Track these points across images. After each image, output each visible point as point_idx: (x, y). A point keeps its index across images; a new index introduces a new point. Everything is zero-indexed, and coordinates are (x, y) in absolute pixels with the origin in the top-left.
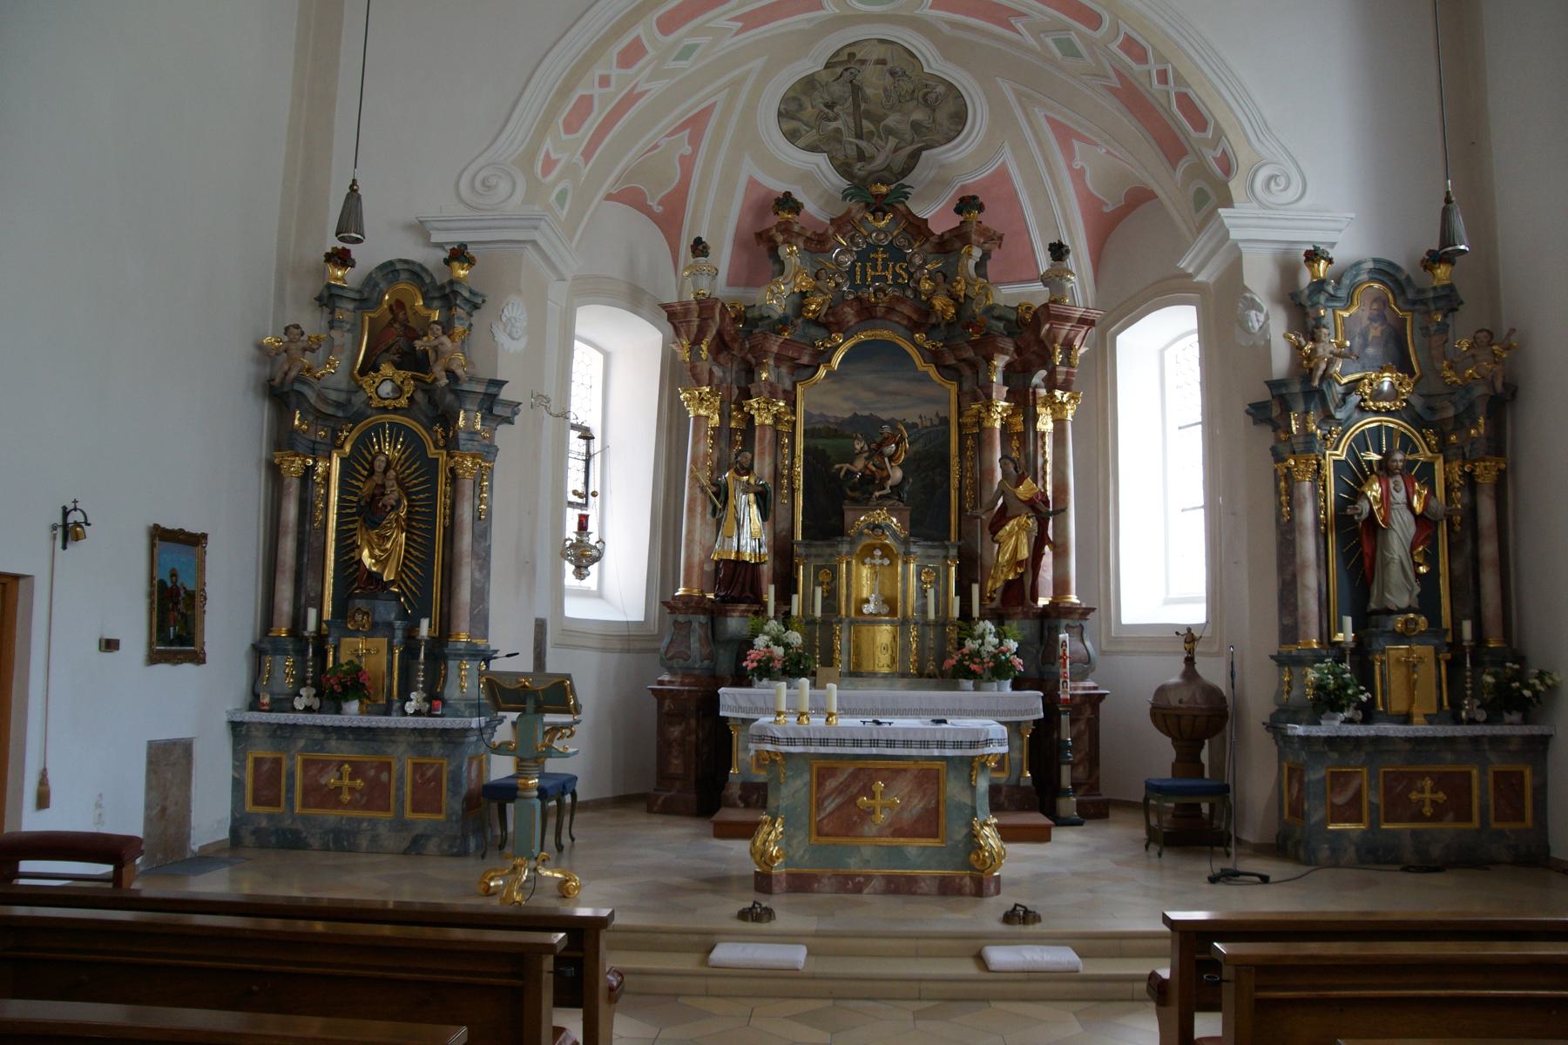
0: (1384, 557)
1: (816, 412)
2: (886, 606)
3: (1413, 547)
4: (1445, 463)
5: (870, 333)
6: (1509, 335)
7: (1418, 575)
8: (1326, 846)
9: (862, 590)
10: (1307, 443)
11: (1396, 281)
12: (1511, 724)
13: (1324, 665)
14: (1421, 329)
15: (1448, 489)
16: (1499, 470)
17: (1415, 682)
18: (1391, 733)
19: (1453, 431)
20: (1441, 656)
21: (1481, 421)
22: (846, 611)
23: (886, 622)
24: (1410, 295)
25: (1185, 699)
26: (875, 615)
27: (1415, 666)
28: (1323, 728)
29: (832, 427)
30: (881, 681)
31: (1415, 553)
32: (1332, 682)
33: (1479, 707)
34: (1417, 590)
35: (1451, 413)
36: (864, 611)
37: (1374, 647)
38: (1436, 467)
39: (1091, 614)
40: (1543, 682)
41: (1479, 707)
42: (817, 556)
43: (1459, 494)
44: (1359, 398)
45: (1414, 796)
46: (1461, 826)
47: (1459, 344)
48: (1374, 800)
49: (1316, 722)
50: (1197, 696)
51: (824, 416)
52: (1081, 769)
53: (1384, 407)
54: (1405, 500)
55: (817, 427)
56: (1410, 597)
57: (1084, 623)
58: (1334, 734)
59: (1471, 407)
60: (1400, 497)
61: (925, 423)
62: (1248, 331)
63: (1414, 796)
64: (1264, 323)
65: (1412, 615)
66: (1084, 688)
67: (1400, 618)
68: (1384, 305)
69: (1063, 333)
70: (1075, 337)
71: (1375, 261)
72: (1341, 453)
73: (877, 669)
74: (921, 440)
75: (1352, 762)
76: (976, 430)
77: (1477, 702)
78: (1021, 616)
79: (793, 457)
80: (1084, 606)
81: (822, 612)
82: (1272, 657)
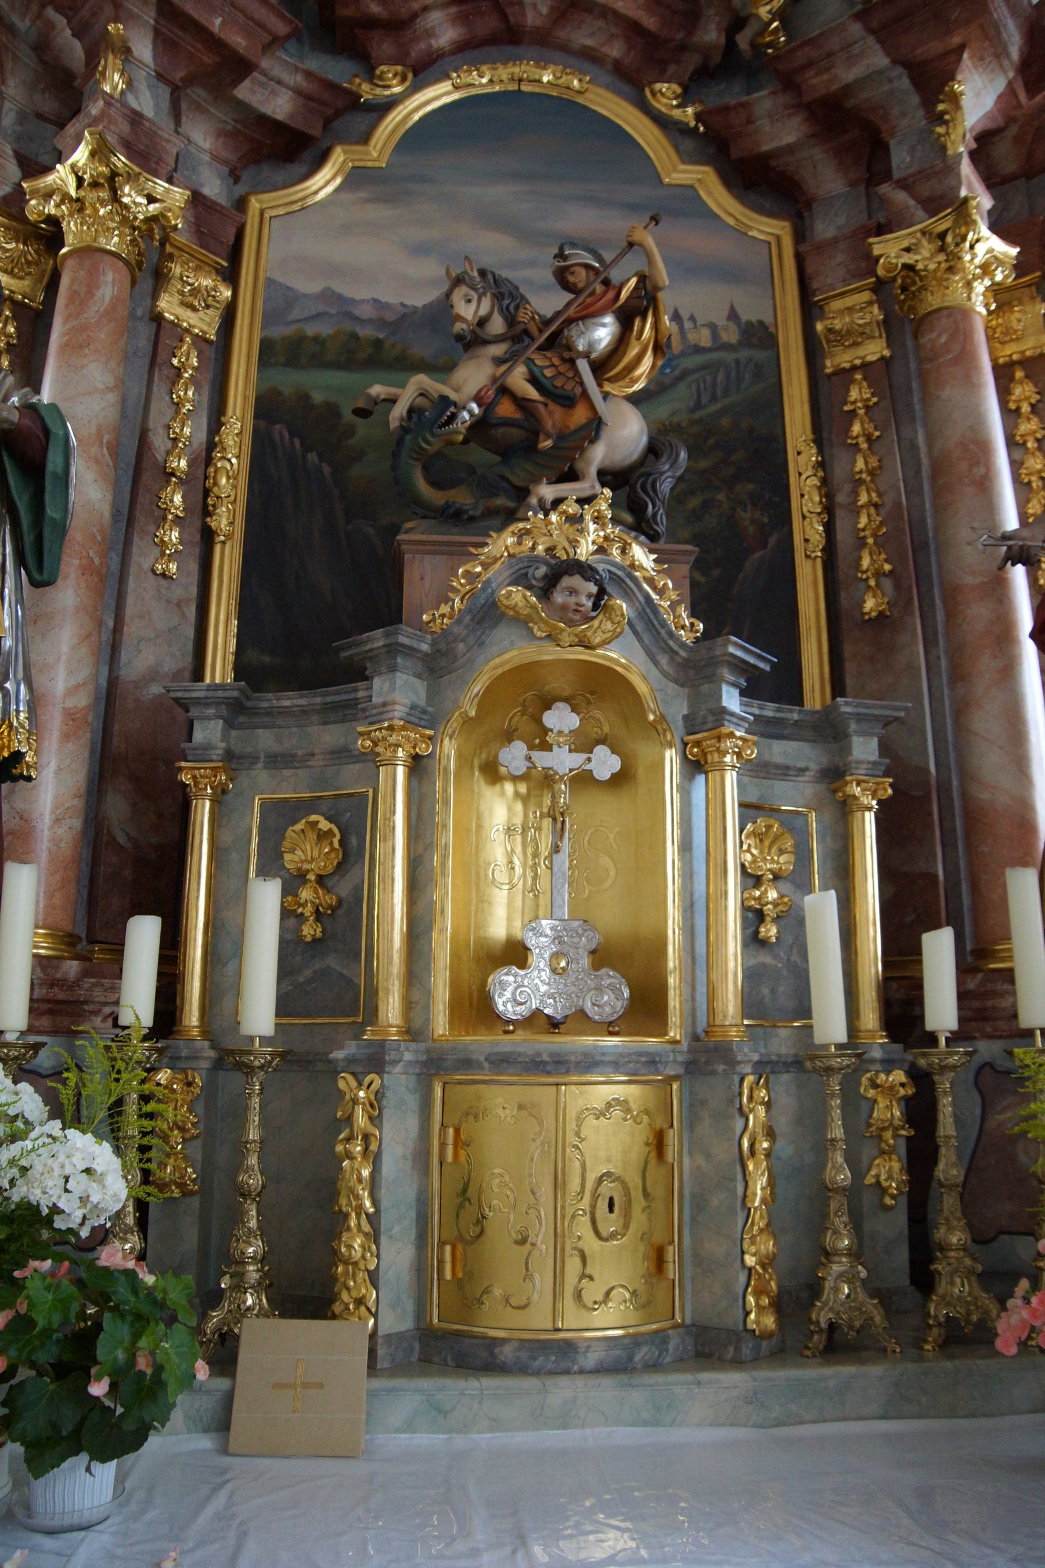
1: (308, 286)
2: (610, 977)
5: (504, 72)
9: (483, 902)
22: (408, 1005)
23: (617, 1063)
26: (554, 1025)
29: (365, 332)
30: (605, 1389)
36: (504, 1004)
42: (277, 761)
51: (340, 297)
55: (311, 330)
61: (692, 337)
73: (571, 1318)
74: (682, 387)
76: (875, 350)
79: (216, 422)
81: (284, 1007)
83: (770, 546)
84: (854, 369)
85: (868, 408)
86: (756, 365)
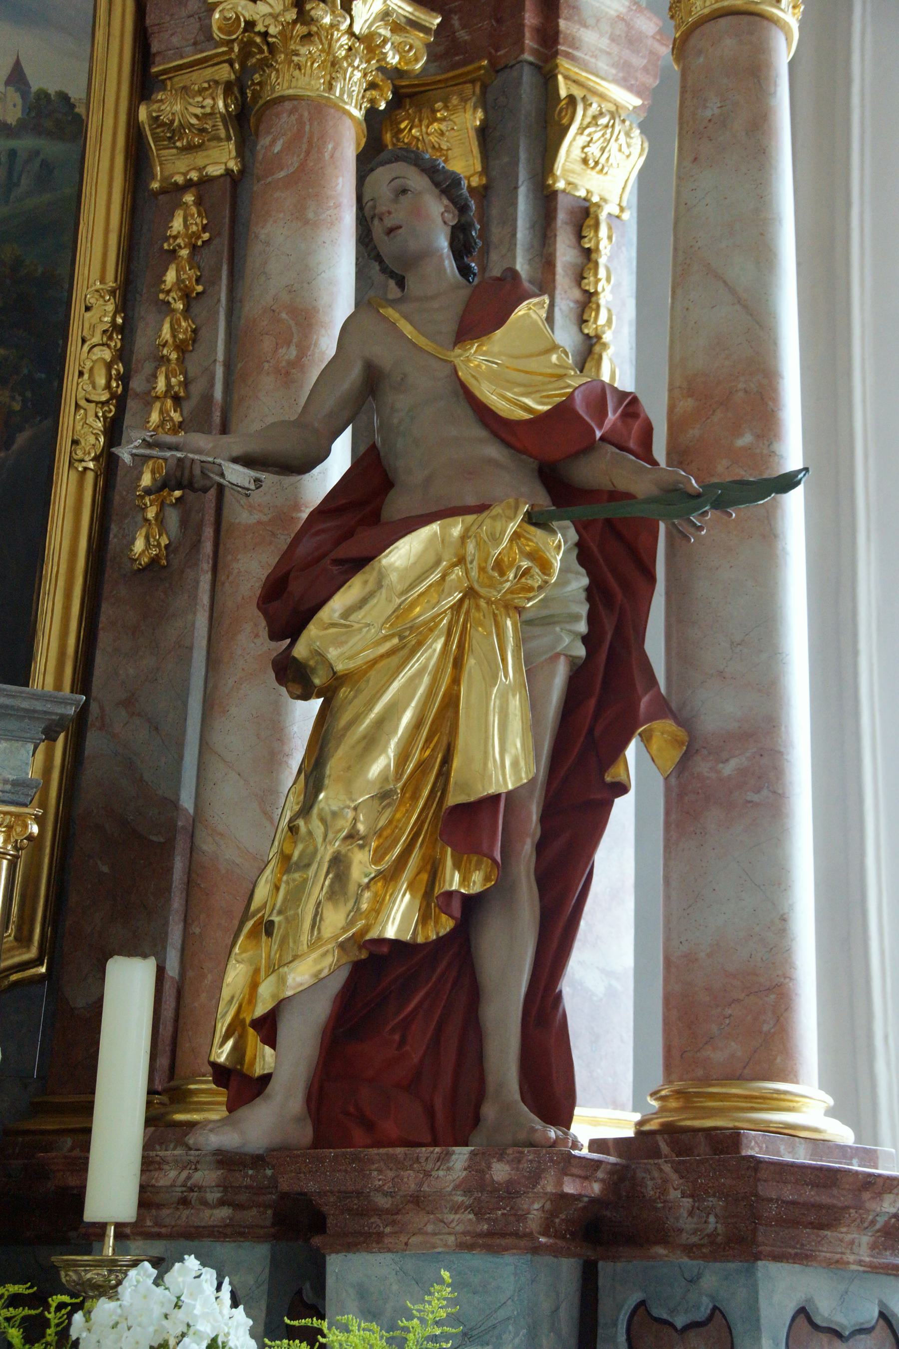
78: (462, 1221)
83: (15, 447)
84: (189, 184)
85: (194, 248)
86: (44, 164)
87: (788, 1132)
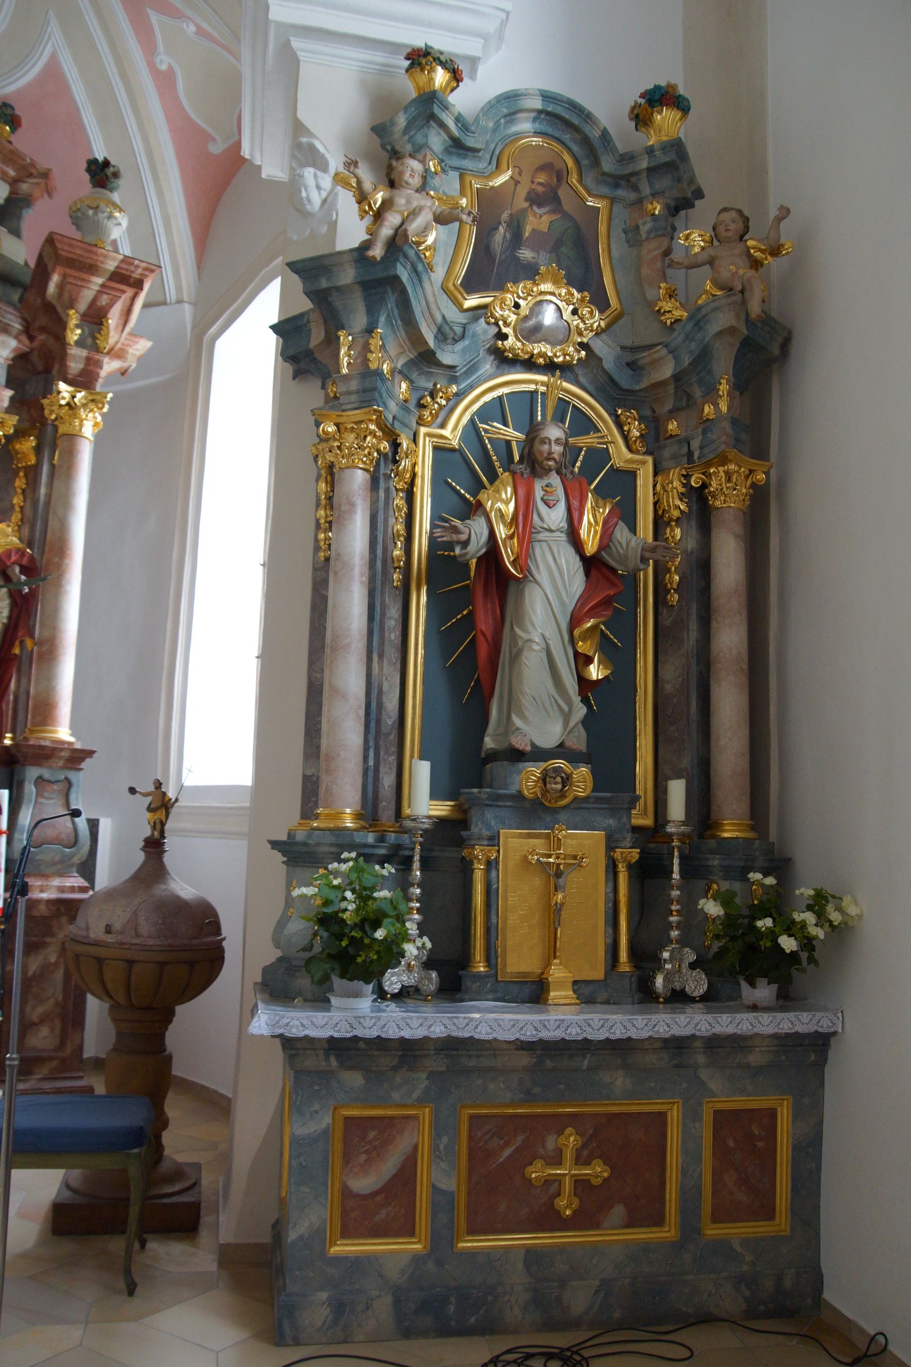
0: (514, 637)
3: (575, 621)
4: (656, 474)
6: (779, 219)
7: (584, 683)
8: (324, 1295)
10: (365, 391)
11: (586, 142)
12: (754, 1008)
13: (344, 867)
14: (625, 232)
15: (660, 523)
16: (754, 485)
17: (559, 908)
18: (483, 1033)
19: (673, 413)
20: (618, 854)
21: (724, 388)
24: (608, 164)
25: (117, 925)
27: (559, 874)
28: (335, 1015)
31: (577, 632)
32: (352, 907)
33: (693, 966)
34: (581, 711)
35: (667, 371)
37: (474, 830)
38: (640, 482)
39: (88, 760)
40: (821, 916)
41: (693, 966)
43: (678, 532)
44: (495, 330)
45: (538, 1171)
46: (642, 1235)
47: (687, 238)
48: (449, 1184)
49: (321, 1001)
50: (142, 920)
52: (44, 1031)
53: (542, 355)
54: (564, 525)
56: (566, 723)
57: (72, 776)
58: (344, 1032)
59: (703, 358)
60: (556, 516)
62: (306, 215)
63: (538, 1171)
64: (330, 193)
65: (560, 763)
66: (61, 889)
67: (534, 770)
68: (559, 178)
69: (86, 296)
70: (111, 305)
71: (546, 96)
72: (452, 433)
75: (396, 1096)
77: (690, 956)
80: (78, 746)
82: (275, 845)
87: (44, 739)
